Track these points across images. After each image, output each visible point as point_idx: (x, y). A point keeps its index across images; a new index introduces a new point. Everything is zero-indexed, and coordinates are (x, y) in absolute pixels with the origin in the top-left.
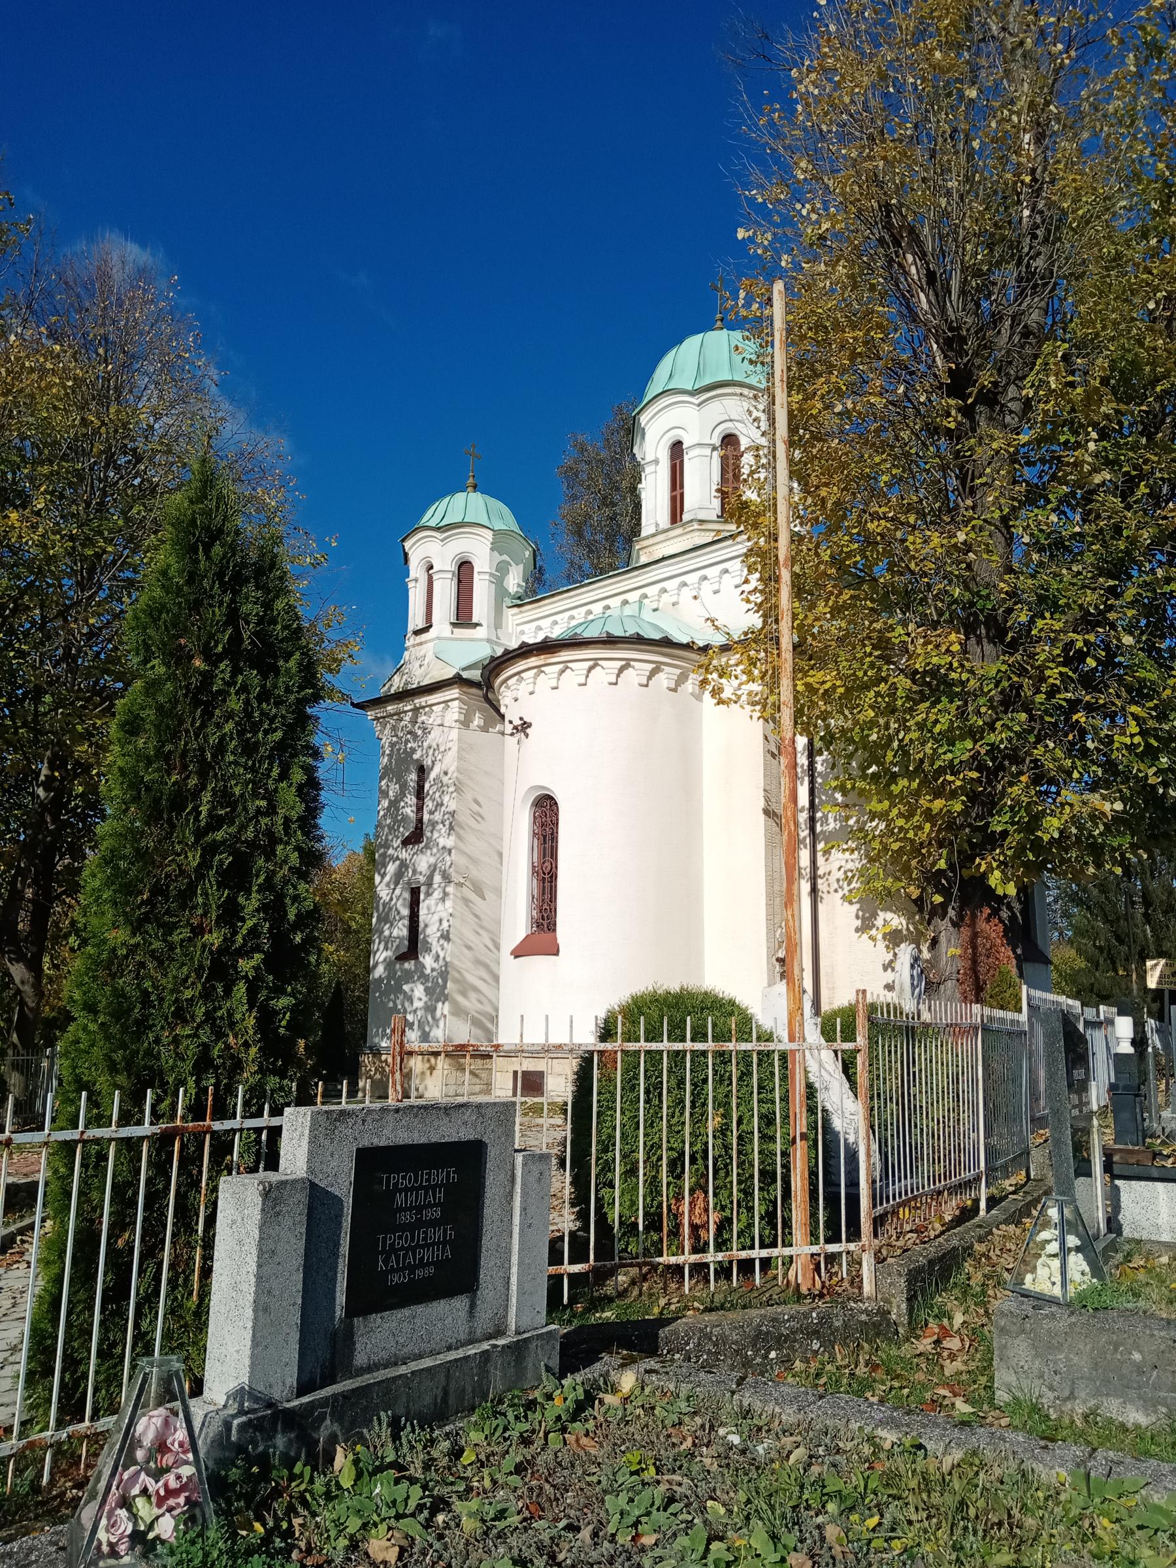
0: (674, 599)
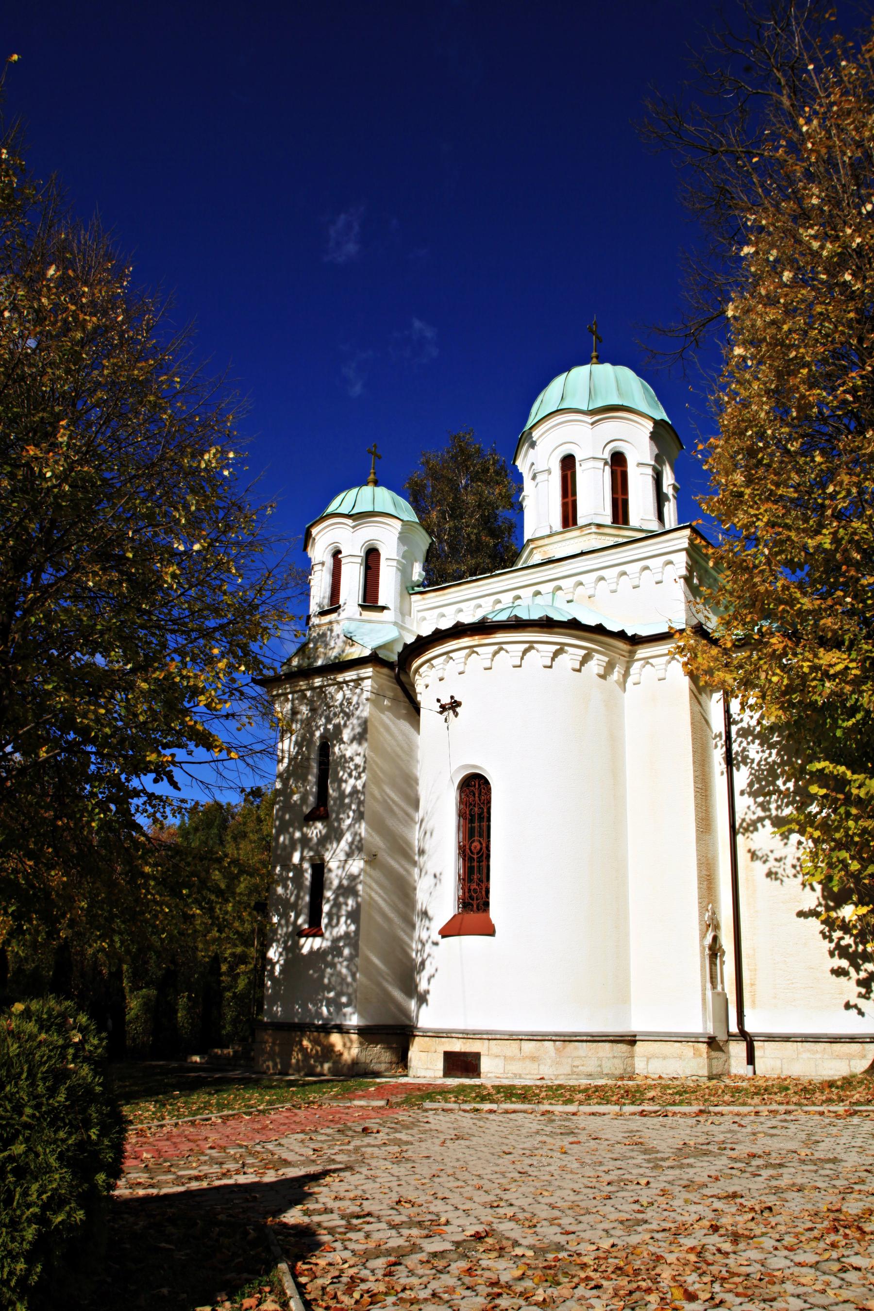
0: (591, 592)
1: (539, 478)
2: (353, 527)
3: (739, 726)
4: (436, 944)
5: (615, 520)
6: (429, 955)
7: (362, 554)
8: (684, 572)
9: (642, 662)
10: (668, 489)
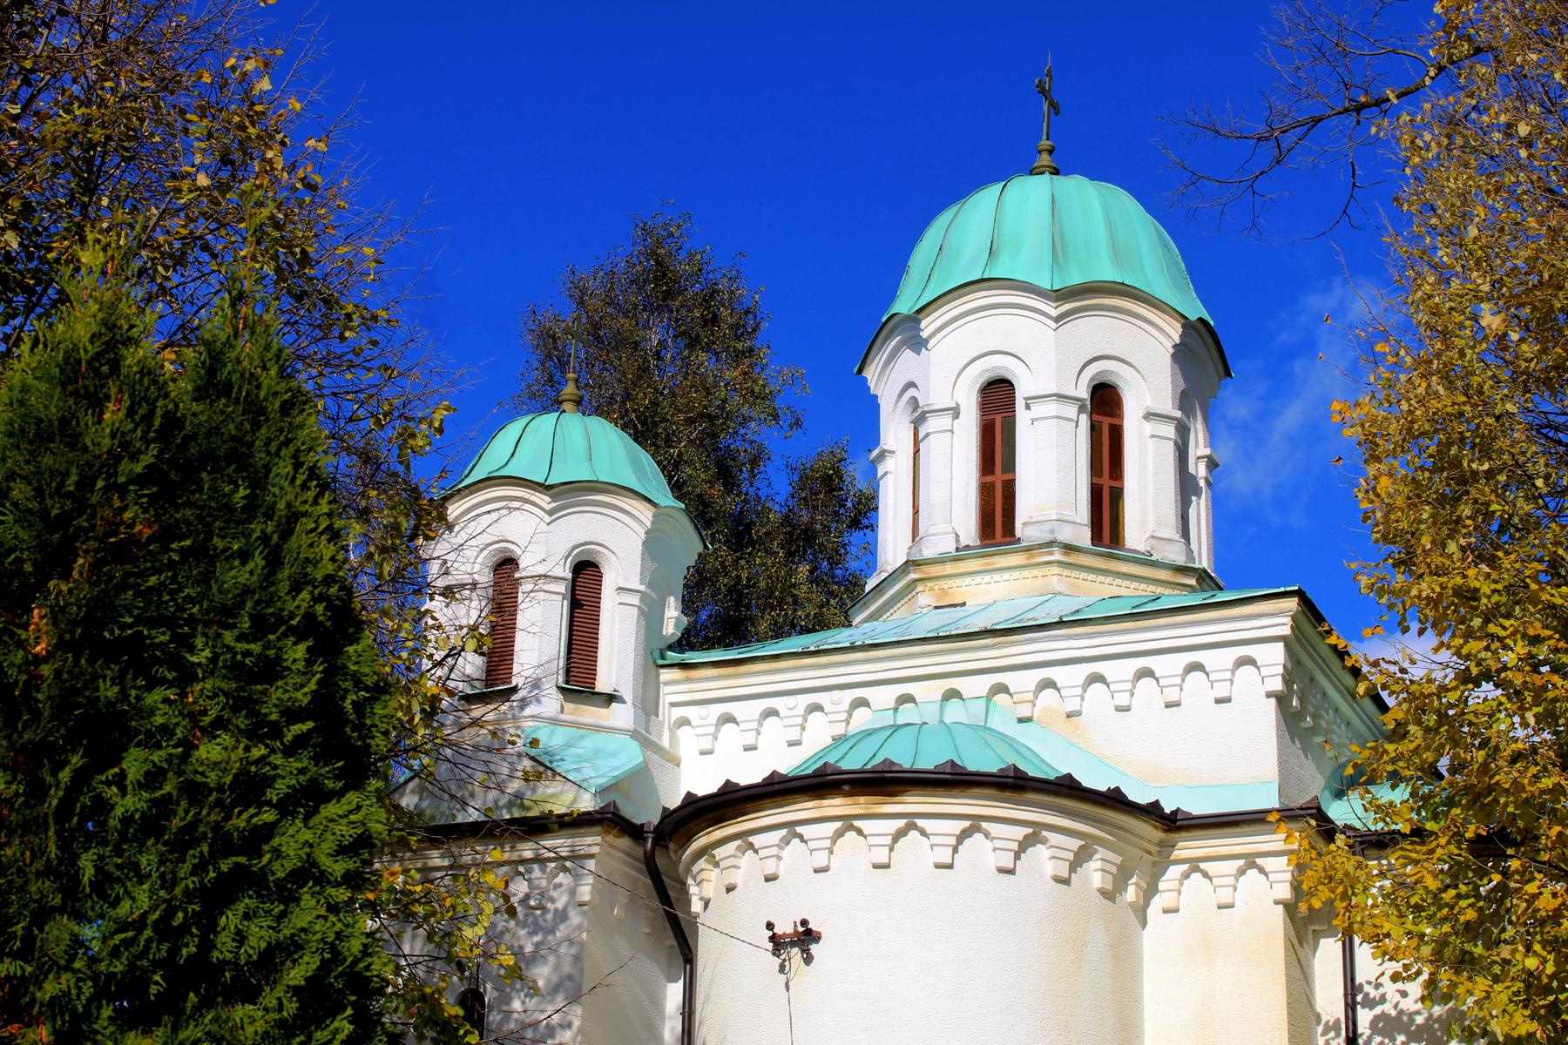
0: (1073, 705)
1: (933, 424)
2: (550, 513)
3: (1378, 1010)
5: (1097, 538)
7: (570, 576)
8: (1277, 685)
9: (1186, 867)
10: (1200, 470)
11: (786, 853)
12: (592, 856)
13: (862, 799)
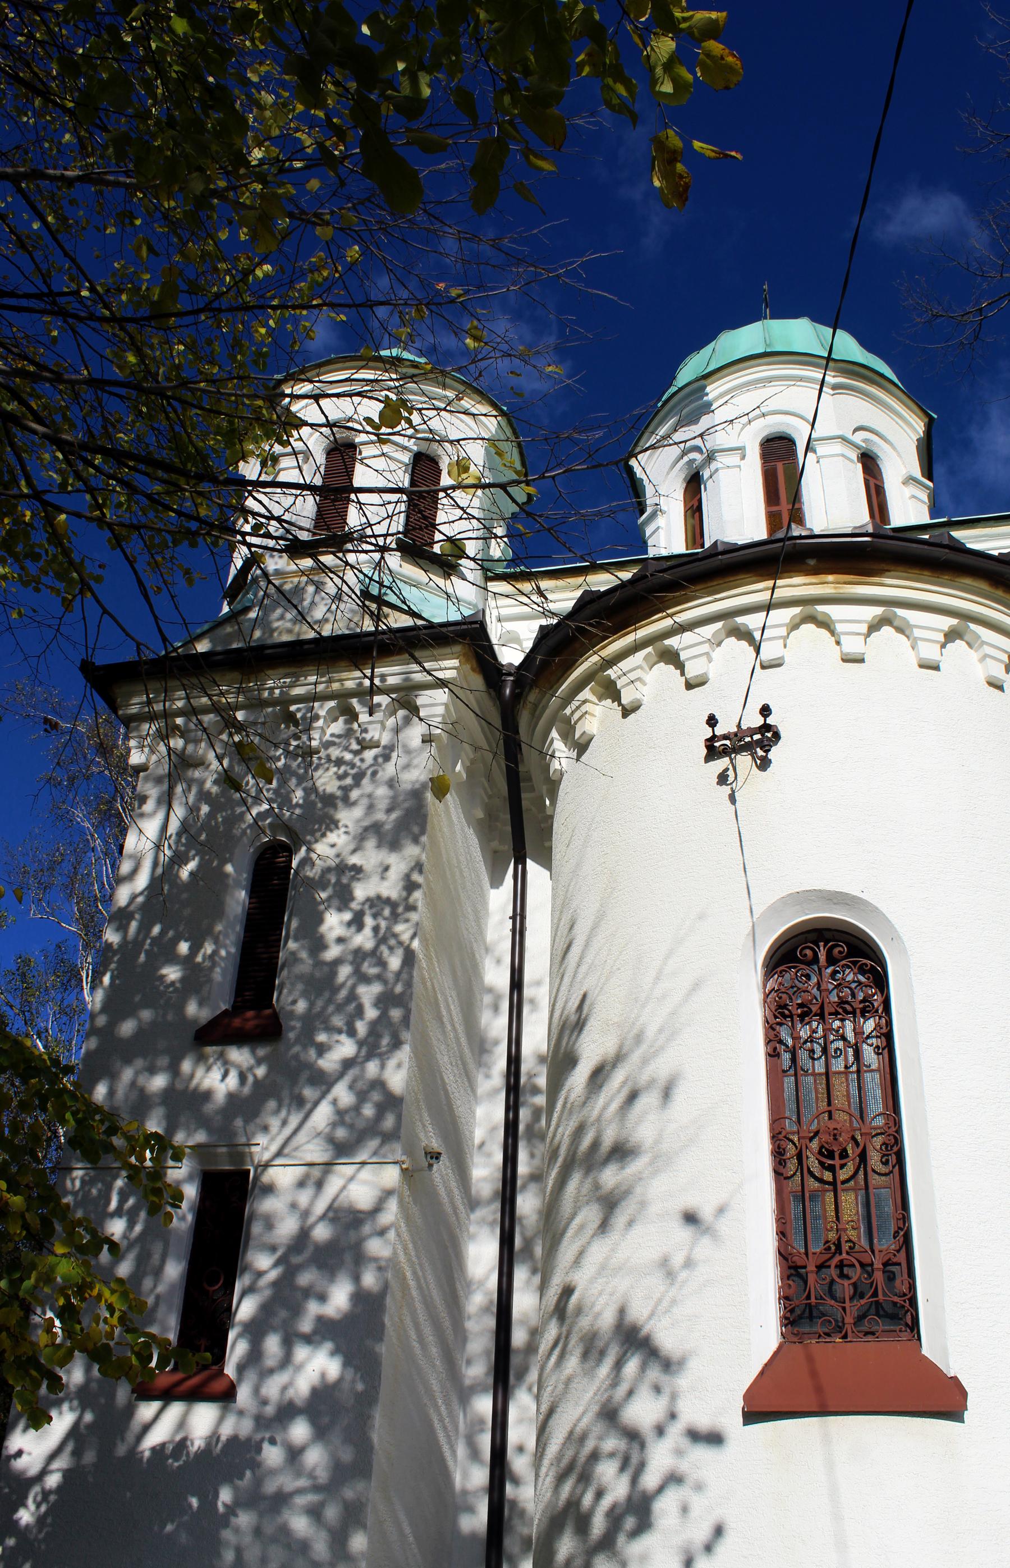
4: (714, 1439)
6: (674, 1479)
11: (717, 653)
12: (442, 683)
13: (830, 578)
